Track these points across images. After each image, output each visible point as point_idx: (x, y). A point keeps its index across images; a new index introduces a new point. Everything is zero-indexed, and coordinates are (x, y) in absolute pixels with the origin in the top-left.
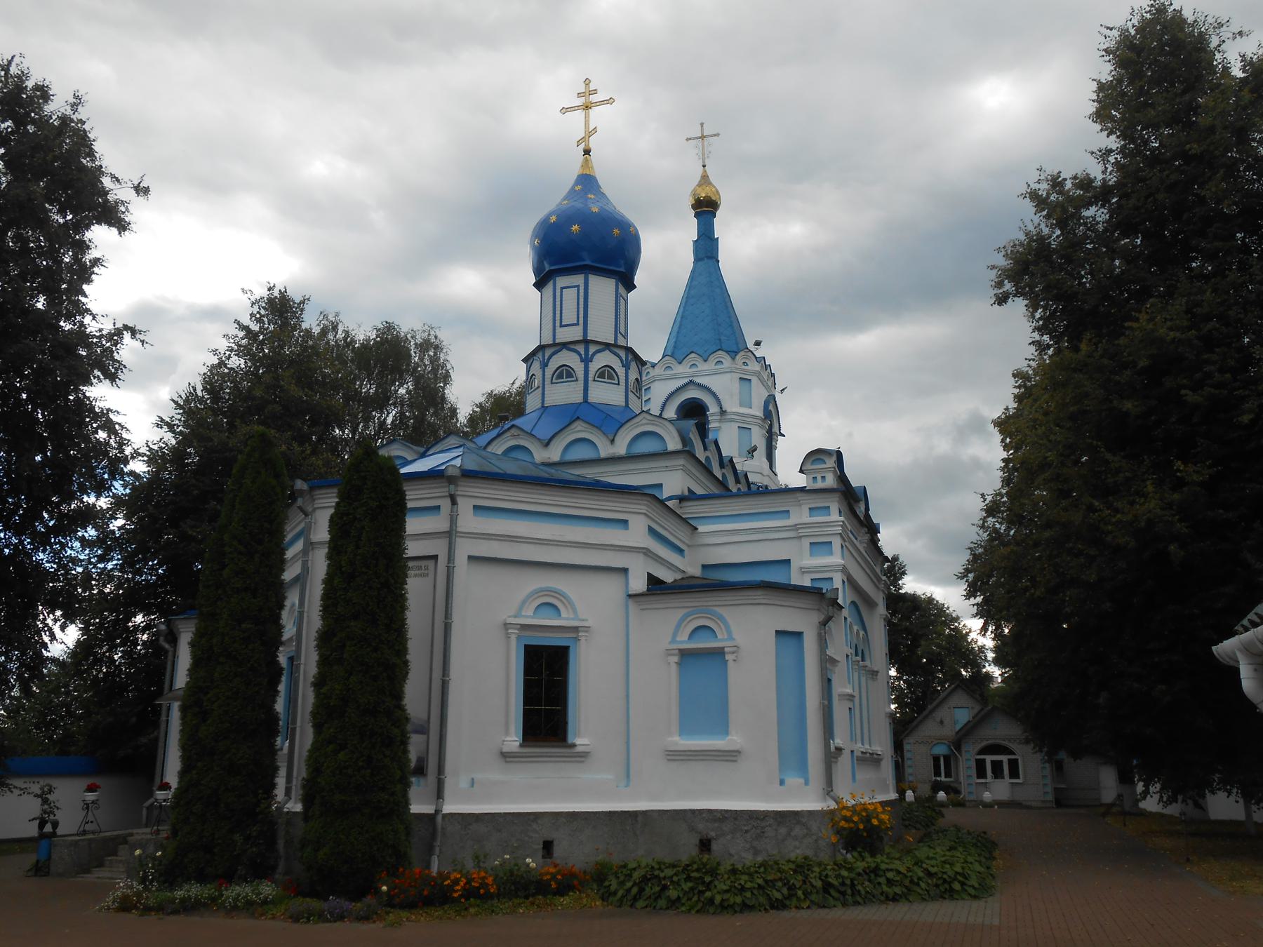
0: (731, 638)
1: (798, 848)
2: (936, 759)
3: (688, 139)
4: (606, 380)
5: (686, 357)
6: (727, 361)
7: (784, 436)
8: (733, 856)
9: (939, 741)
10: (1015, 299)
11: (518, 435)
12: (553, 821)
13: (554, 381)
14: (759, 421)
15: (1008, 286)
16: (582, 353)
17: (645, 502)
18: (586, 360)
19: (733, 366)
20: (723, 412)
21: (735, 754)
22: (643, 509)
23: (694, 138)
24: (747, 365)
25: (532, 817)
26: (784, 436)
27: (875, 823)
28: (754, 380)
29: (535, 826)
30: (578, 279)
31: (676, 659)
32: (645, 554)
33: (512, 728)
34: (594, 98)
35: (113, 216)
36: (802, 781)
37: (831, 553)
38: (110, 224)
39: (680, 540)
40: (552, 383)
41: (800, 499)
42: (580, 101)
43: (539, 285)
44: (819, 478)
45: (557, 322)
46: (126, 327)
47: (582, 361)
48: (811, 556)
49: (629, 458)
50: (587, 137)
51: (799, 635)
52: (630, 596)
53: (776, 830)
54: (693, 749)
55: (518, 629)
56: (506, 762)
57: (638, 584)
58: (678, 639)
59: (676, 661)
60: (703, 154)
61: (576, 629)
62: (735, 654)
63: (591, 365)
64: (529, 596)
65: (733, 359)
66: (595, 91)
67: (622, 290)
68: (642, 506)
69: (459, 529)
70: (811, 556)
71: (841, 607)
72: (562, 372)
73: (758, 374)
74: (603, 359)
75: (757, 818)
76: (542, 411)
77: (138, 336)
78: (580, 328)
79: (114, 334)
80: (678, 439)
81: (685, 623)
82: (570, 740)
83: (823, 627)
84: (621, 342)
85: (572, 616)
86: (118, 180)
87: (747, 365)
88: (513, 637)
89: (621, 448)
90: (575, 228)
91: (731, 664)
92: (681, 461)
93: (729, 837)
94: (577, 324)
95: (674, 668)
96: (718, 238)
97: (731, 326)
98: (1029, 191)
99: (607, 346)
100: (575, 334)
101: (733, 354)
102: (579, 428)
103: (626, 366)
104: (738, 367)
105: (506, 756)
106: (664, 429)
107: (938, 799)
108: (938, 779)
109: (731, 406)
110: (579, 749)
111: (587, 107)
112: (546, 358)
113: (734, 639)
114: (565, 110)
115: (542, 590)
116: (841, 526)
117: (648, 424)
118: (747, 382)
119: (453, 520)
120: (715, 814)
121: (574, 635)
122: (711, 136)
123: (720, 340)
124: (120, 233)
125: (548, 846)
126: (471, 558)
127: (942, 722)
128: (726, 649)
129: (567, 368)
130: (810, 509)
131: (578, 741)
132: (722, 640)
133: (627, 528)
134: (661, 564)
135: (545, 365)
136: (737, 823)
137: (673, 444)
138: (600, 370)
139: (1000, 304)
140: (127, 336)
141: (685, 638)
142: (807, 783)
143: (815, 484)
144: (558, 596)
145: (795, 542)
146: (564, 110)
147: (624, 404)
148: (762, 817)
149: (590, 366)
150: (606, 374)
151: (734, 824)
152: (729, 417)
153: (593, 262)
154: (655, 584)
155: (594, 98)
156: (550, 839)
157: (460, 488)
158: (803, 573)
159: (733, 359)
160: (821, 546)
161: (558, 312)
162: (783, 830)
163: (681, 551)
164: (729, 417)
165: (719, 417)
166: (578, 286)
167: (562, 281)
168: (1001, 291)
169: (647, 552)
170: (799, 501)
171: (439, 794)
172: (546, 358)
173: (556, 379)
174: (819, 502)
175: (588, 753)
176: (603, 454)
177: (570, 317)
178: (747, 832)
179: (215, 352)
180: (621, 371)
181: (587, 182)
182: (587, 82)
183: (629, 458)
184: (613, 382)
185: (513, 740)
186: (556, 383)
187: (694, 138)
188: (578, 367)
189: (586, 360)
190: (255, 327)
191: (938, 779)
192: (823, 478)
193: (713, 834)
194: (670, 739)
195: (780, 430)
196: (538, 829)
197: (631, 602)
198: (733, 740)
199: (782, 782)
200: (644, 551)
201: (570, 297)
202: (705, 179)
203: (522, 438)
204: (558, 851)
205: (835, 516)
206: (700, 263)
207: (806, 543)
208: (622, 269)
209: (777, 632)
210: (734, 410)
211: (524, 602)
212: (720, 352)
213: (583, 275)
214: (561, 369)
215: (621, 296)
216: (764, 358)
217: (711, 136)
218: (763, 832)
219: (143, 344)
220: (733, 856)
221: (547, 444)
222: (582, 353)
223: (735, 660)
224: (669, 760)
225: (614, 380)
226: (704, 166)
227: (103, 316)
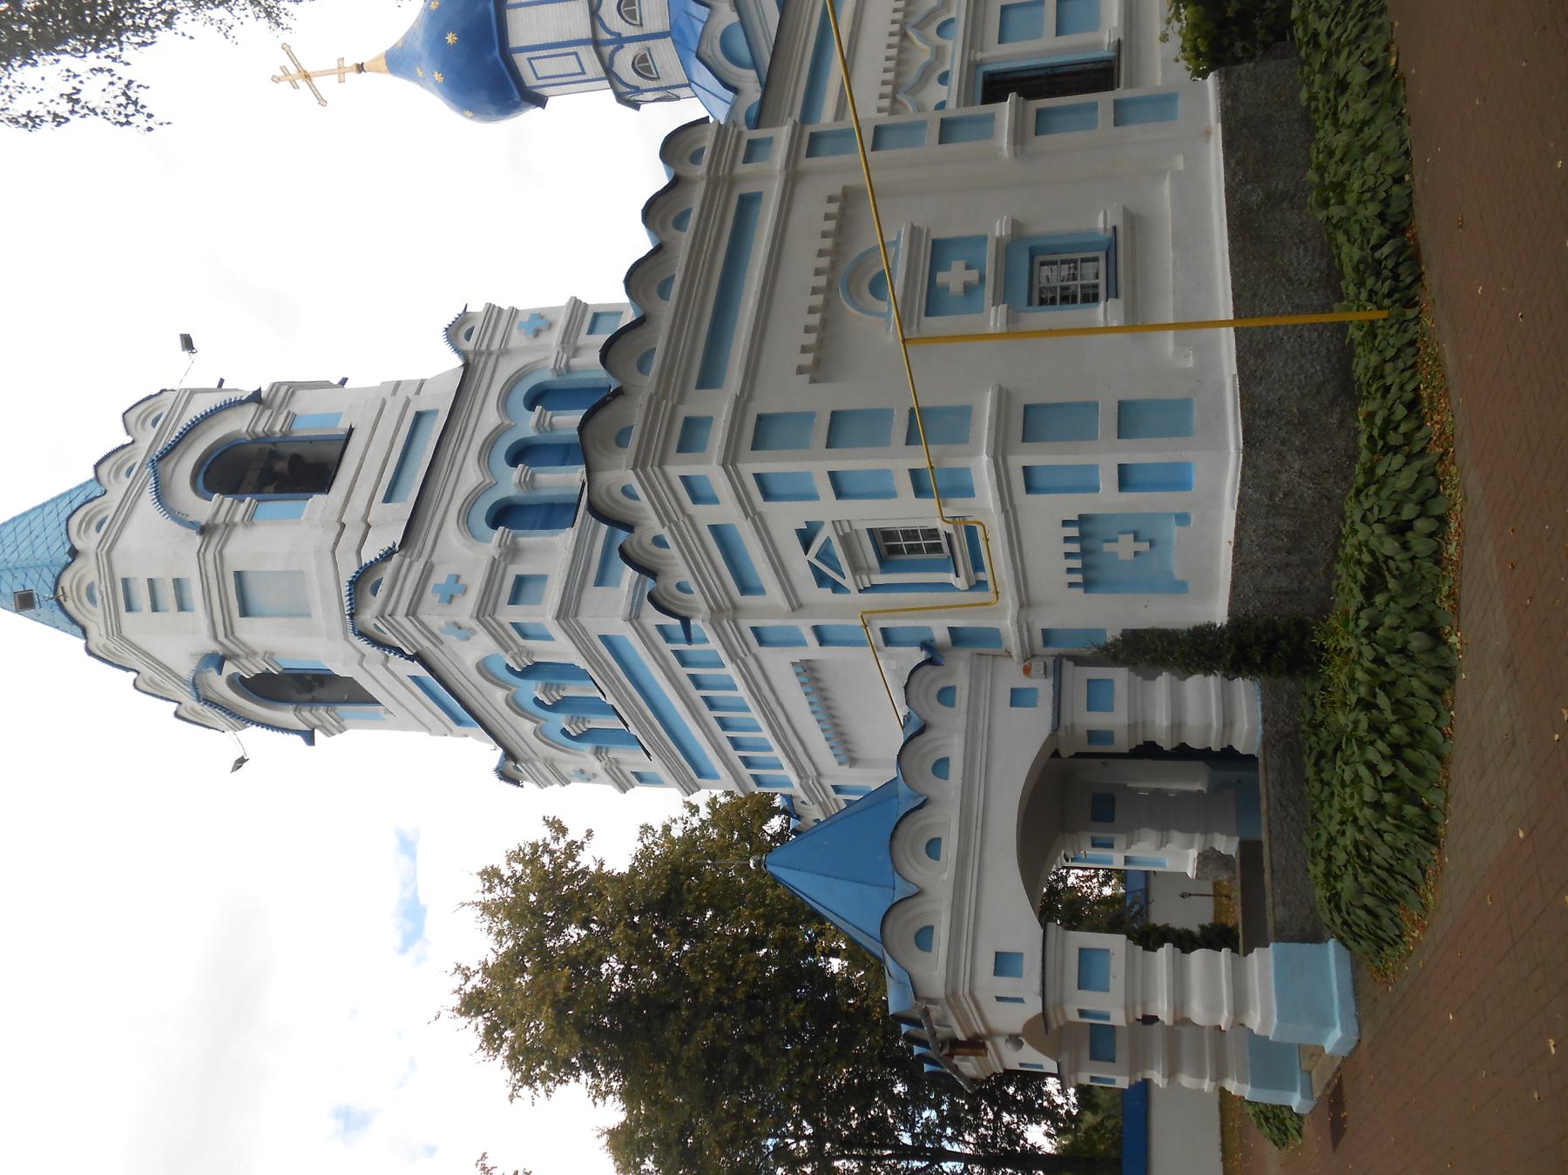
4: (636, 7)
16: (611, 47)
18: (620, 41)
30: (521, 60)
34: (292, 69)
40: (659, 78)
42: (301, 83)
43: (540, 101)
45: (578, 79)
47: (622, 47)
63: (624, 35)
66: (283, 69)
72: (642, 68)
76: (693, 84)
78: (581, 50)
94: (576, 54)
100: (588, 54)
111: (307, 77)
114: (322, 102)
135: (638, 90)
155: (292, 69)
166: (530, 60)
167: (530, 80)
177: (571, 65)
181: (397, 62)
182: (276, 79)
189: (620, 41)
201: (546, 67)
208: (491, 6)
213: (507, 11)
222: (611, 47)
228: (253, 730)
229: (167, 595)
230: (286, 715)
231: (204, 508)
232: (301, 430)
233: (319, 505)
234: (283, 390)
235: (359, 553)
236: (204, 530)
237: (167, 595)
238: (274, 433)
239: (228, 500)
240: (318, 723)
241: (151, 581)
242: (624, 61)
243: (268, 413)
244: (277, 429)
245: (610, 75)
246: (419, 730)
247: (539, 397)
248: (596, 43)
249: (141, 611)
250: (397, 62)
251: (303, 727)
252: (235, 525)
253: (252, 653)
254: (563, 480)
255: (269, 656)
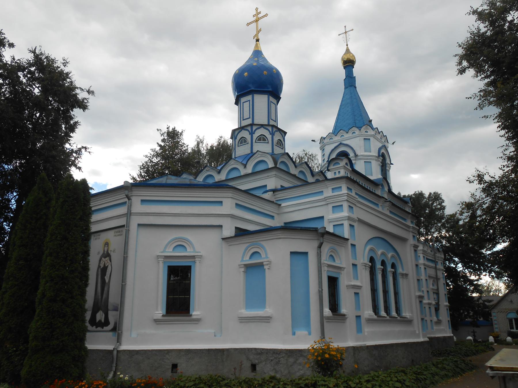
0: (267, 257)
1: (302, 370)
2: (510, 320)
3: (339, 35)
4: (262, 142)
5: (338, 133)
6: (357, 131)
7: (393, 164)
8: (266, 374)
9: (510, 311)
10: (469, 69)
11: (209, 170)
12: (178, 354)
13: (239, 145)
14: (375, 158)
15: (465, 63)
16: (250, 130)
17: (231, 192)
18: (252, 133)
19: (360, 133)
20: (356, 156)
21: (268, 318)
22: (230, 195)
23: (342, 34)
24: (368, 132)
25: (166, 352)
26: (393, 164)
27: (327, 357)
28: (372, 139)
29: (167, 356)
30: (249, 97)
31: (243, 269)
32: (231, 217)
33: (160, 307)
34: (260, 16)
35: (82, 105)
36: (306, 332)
37: (342, 211)
38: (80, 108)
39: (273, 212)
40: (238, 146)
41: (327, 184)
42: (255, 18)
44: (337, 173)
45: (241, 118)
46: (83, 147)
48: (333, 213)
49: (253, 174)
50: (257, 34)
51: (306, 253)
52: (223, 239)
53: (287, 360)
54: (249, 316)
55: (164, 259)
56: (157, 324)
57: (229, 231)
58: (244, 259)
59: (243, 271)
60: (347, 40)
61: (193, 257)
62: (269, 266)
64: (169, 242)
65: (360, 130)
67: (272, 99)
68: (229, 193)
69: (132, 212)
70: (333, 213)
71: (348, 239)
73: (373, 136)
74: (261, 131)
75: (277, 353)
77: (87, 150)
78: (251, 119)
79: (78, 151)
80: (272, 162)
81: (247, 251)
82: (191, 313)
83: (319, 249)
84: (272, 123)
85: (192, 251)
86: (83, 90)
87: (368, 132)
88: (161, 262)
89: (249, 170)
90: (246, 74)
91: (267, 270)
92: (274, 173)
93: (264, 363)
95: (242, 274)
96: (355, 77)
97: (361, 115)
98: (472, 10)
99: (262, 126)
100: (249, 122)
101: (360, 128)
102: (233, 163)
103: (273, 134)
104: (362, 133)
105: (156, 321)
106: (267, 158)
107: (507, 341)
108: (512, 330)
109: (360, 152)
110: (194, 317)
111: (257, 21)
112: (236, 135)
113: (268, 258)
114: (248, 24)
115: (176, 239)
116: (347, 196)
117: (260, 157)
118: (368, 140)
119: (129, 209)
120: (258, 351)
121: (193, 260)
122: (349, 31)
123: (355, 122)
124: (84, 111)
125: (175, 366)
126: (139, 225)
127: (511, 301)
128: (264, 263)
129: (244, 138)
130: (333, 189)
131: (193, 314)
132: (264, 258)
133: (222, 205)
134: (247, 222)
135: (236, 138)
136: (268, 355)
137: (271, 165)
138: (259, 137)
139: (461, 74)
140: (83, 150)
141: (248, 258)
142: (310, 334)
143: (335, 176)
144: (185, 241)
145: (326, 206)
146: (248, 24)
147: (271, 152)
148: (279, 353)
149: (253, 136)
150: (262, 139)
151: (266, 356)
152: (359, 157)
153: (255, 88)
154: (241, 233)
155: (260, 16)
156: (175, 363)
157: (133, 192)
158: (330, 222)
159: (360, 130)
160: (337, 208)
161: (242, 114)
162: (291, 360)
163: (272, 217)
164: (359, 157)
165: (354, 158)
166: (249, 101)
167: (243, 100)
168: (461, 67)
169: (232, 216)
170: (327, 185)
171: (119, 340)
172: (236, 135)
173: (240, 144)
174: (336, 185)
175: (200, 319)
176: (242, 174)
177: (246, 115)
178: (272, 360)
179: (146, 156)
180: (269, 137)
182: (257, 9)
183: (253, 174)
184: (265, 142)
185: (160, 311)
186: (240, 146)
187: (342, 34)
188: (248, 137)
189: (252, 133)
190: (163, 144)
191: (512, 330)
192: (339, 172)
193: (257, 361)
194: (240, 311)
195: (391, 162)
196: (169, 358)
197: (223, 242)
198: (268, 311)
199: (294, 334)
200: (231, 216)
202: (348, 51)
203: (210, 171)
204: (180, 369)
205: (344, 191)
206: (347, 89)
207: (330, 206)
208: (270, 90)
209: (291, 253)
210: (362, 154)
211: (167, 245)
212: (354, 128)
214: (242, 139)
215: (271, 102)
216: (377, 128)
217: (349, 31)
218: (279, 361)
219: (90, 153)
220: (266, 374)
221: (219, 172)
222: (250, 130)
223: (269, 269)
224: (240, 322)
225: (266, 141)
226: (347, 45)
227: (73, 144)
242: (245, 134)
245: (241, 128)
248: (252, 125)
250: (257, 53)
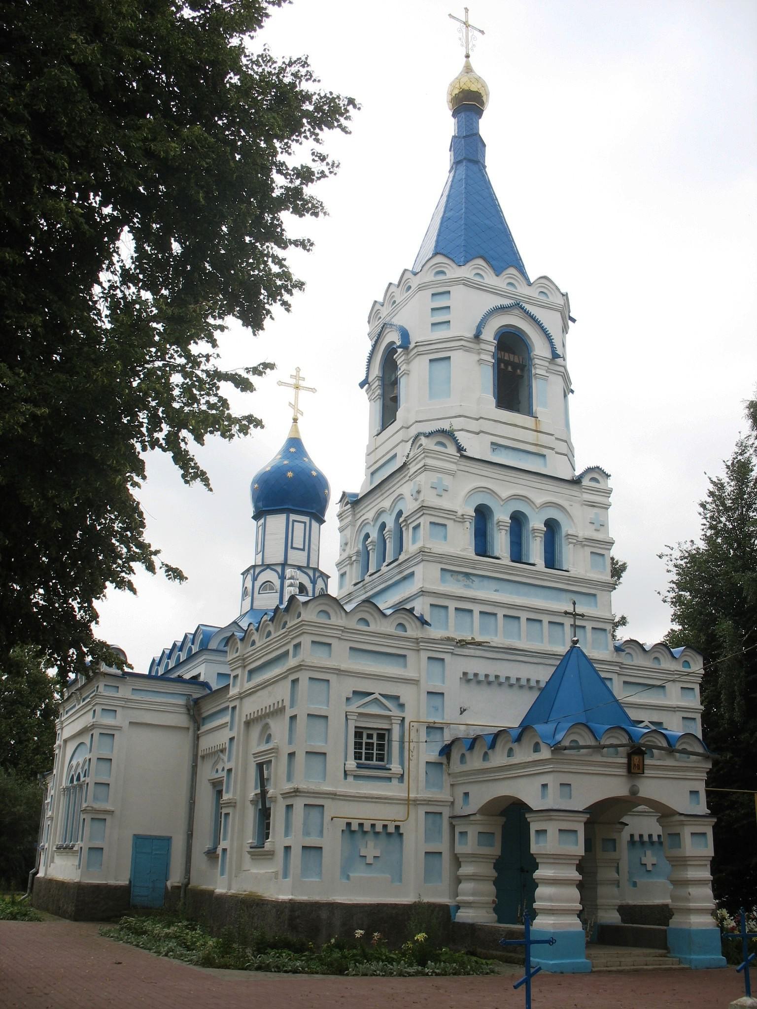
228: (368, 346)
229: (440, 317)
230: (376, 371)
231: (489, 334)
232: (536, 385)
233: (492, 401)
234: (562, 369)
235: (462, 430)
236: (477, 337)
237: (440, 317)
238: (535, 368)
239: (492, 349)
240: (373, 387)
241: (449, 307)
243: (547, 364)
244: (538, 371)
246: (368, 446)
247: (552, 526)
249: (432, 301)
251: (370, 380)
252: (479, 354)
253: (408, 362)
254: (501, 543)
255: (407, 373)
